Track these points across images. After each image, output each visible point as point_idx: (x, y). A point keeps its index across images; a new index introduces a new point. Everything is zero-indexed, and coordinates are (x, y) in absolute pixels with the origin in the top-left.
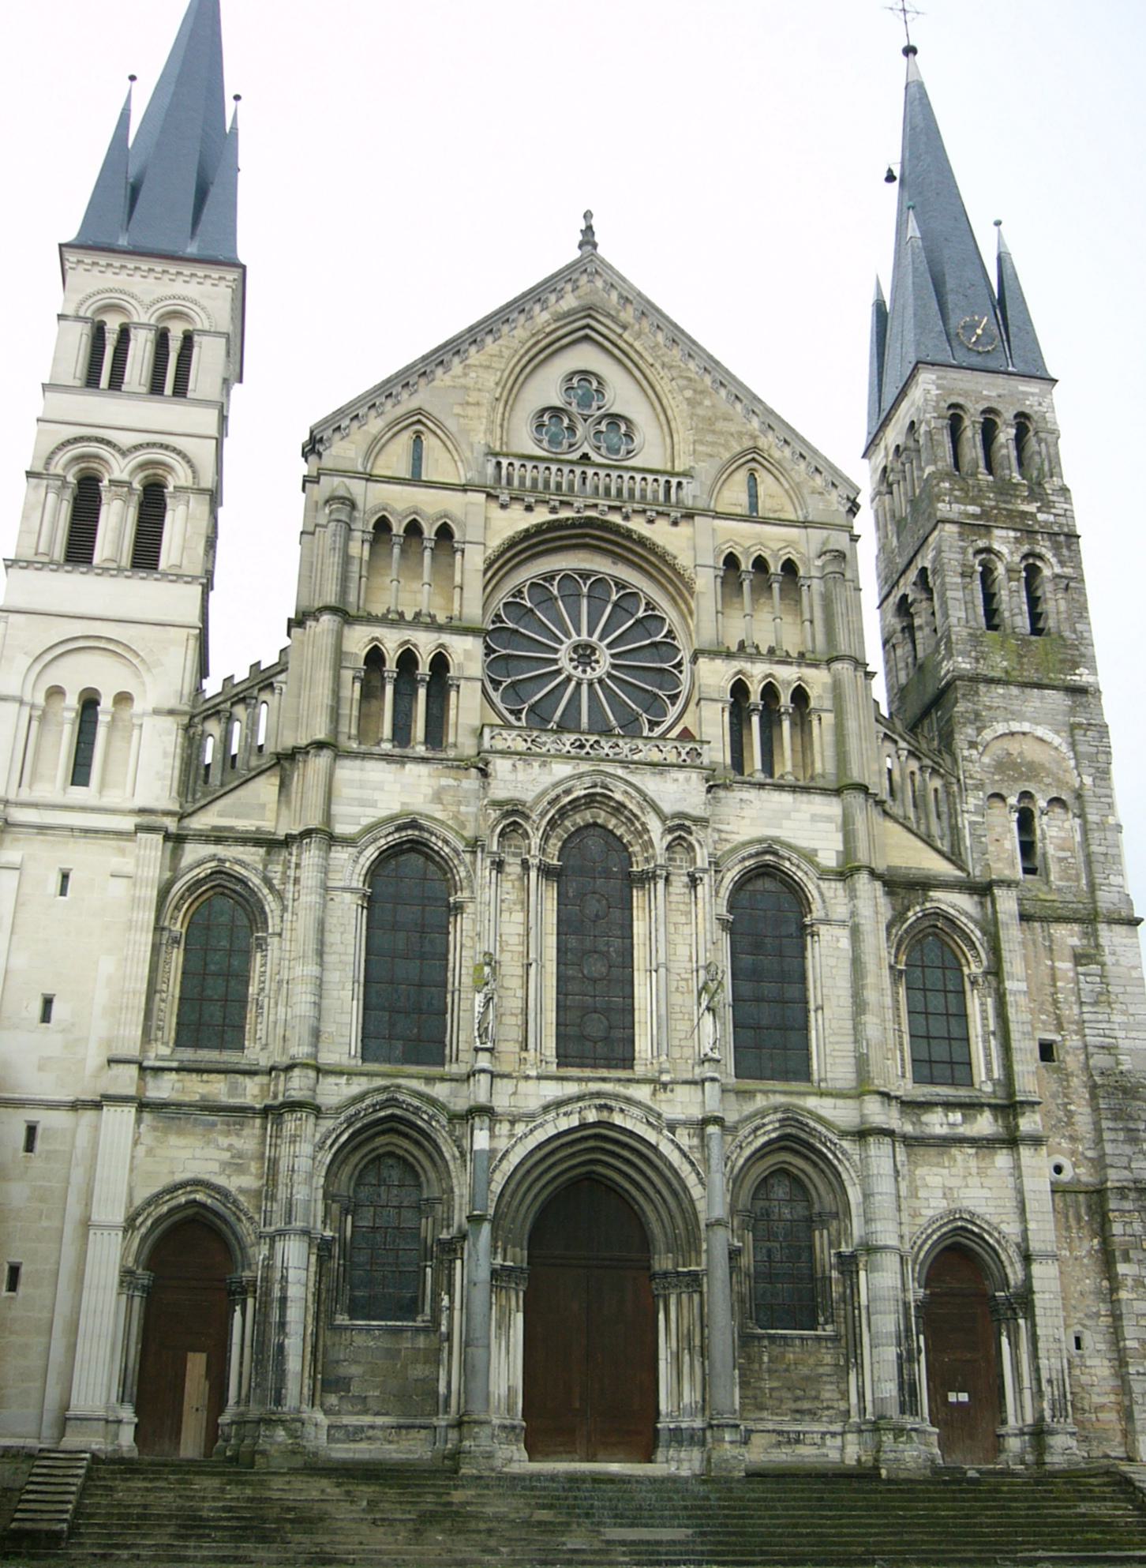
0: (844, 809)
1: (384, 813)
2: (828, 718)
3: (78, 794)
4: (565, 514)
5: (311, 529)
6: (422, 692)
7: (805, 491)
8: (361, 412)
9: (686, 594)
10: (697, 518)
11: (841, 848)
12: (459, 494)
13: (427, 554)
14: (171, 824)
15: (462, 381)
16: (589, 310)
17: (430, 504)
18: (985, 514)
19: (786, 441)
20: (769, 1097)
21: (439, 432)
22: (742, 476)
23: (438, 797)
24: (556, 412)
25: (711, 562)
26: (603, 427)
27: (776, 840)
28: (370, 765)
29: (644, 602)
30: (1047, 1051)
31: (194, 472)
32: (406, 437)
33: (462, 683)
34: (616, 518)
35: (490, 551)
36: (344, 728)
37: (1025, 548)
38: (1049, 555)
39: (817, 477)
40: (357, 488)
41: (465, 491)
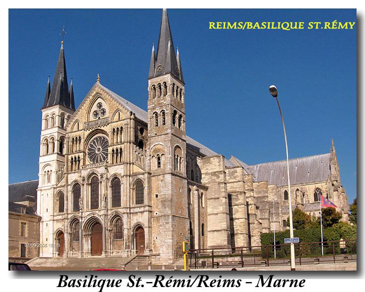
3: (49, 184)
4: (94, 129)
14: (55, 186)
16: (97, 93)
17: (78, 134)
18: (155, 105)
20: (115, 209)
30: (157, 196)
32: (77, 124)
34: (99, 128)
37: (161, 110)
38: (165, 109)
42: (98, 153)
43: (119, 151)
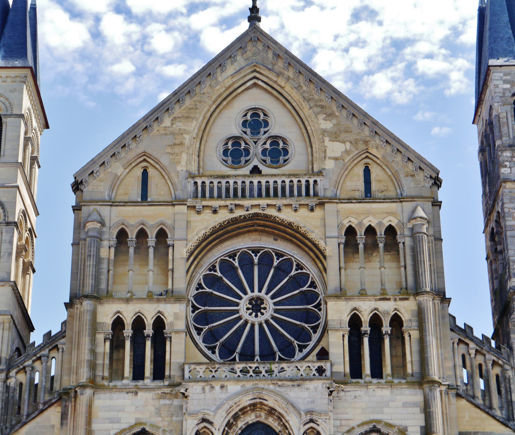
0: (425, 397)
1: (125, 426)
2: (415, 334)
4: (239, 213)
5: (77, 241)
6: (148, 344)
7: (402, 176)
8: (105, 160)
9: (321, 257)
10: (326, 205)
11: (423, 424)
12: (170, 208)
13: (151, 250)
15: (171, 129)
19: (387, 142)
21: (157, 166)
22: (360, 170)
23: (158, 413)
24: (236, 140)
25: (336, 234)
26: (268, 146)
27: (379, 421)
28: (116, 395)
29: (295, 264)
31: (4, 212)
32: (138, 172)
33: (173, 336)
34: (272, 212)
35: (190, 244)
36: (99, 373)
39: (410, 164)
40: (105, 211)
41: (174, 205)
42: (252, 319)
43: (386, 328)
